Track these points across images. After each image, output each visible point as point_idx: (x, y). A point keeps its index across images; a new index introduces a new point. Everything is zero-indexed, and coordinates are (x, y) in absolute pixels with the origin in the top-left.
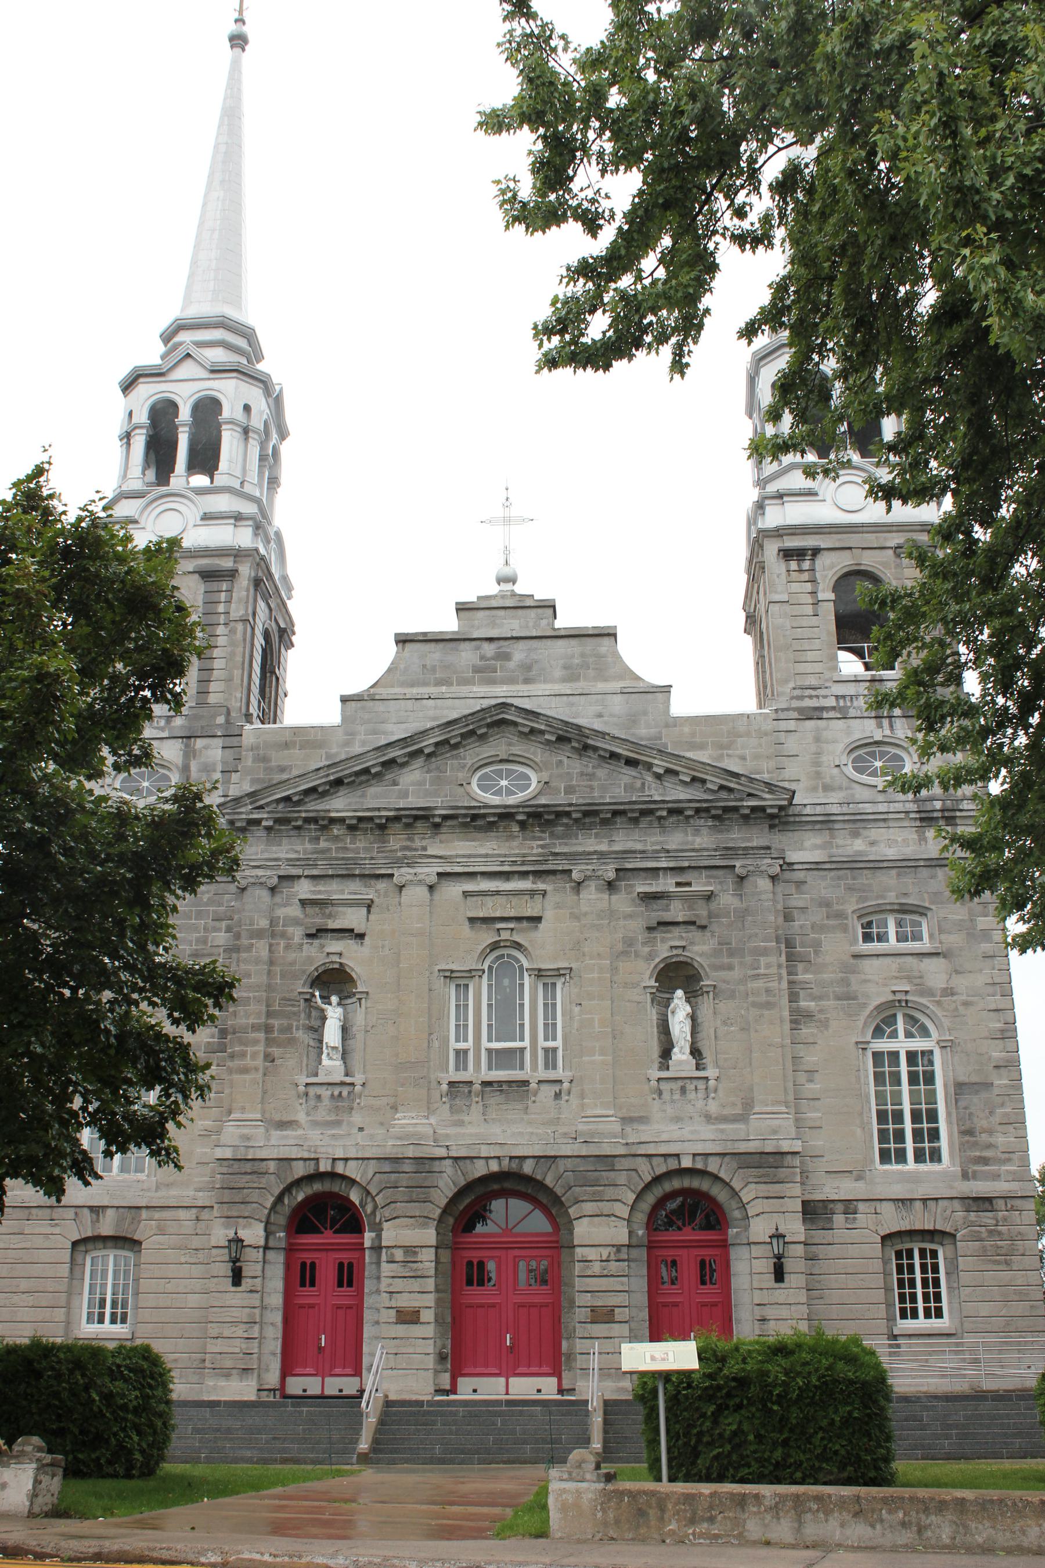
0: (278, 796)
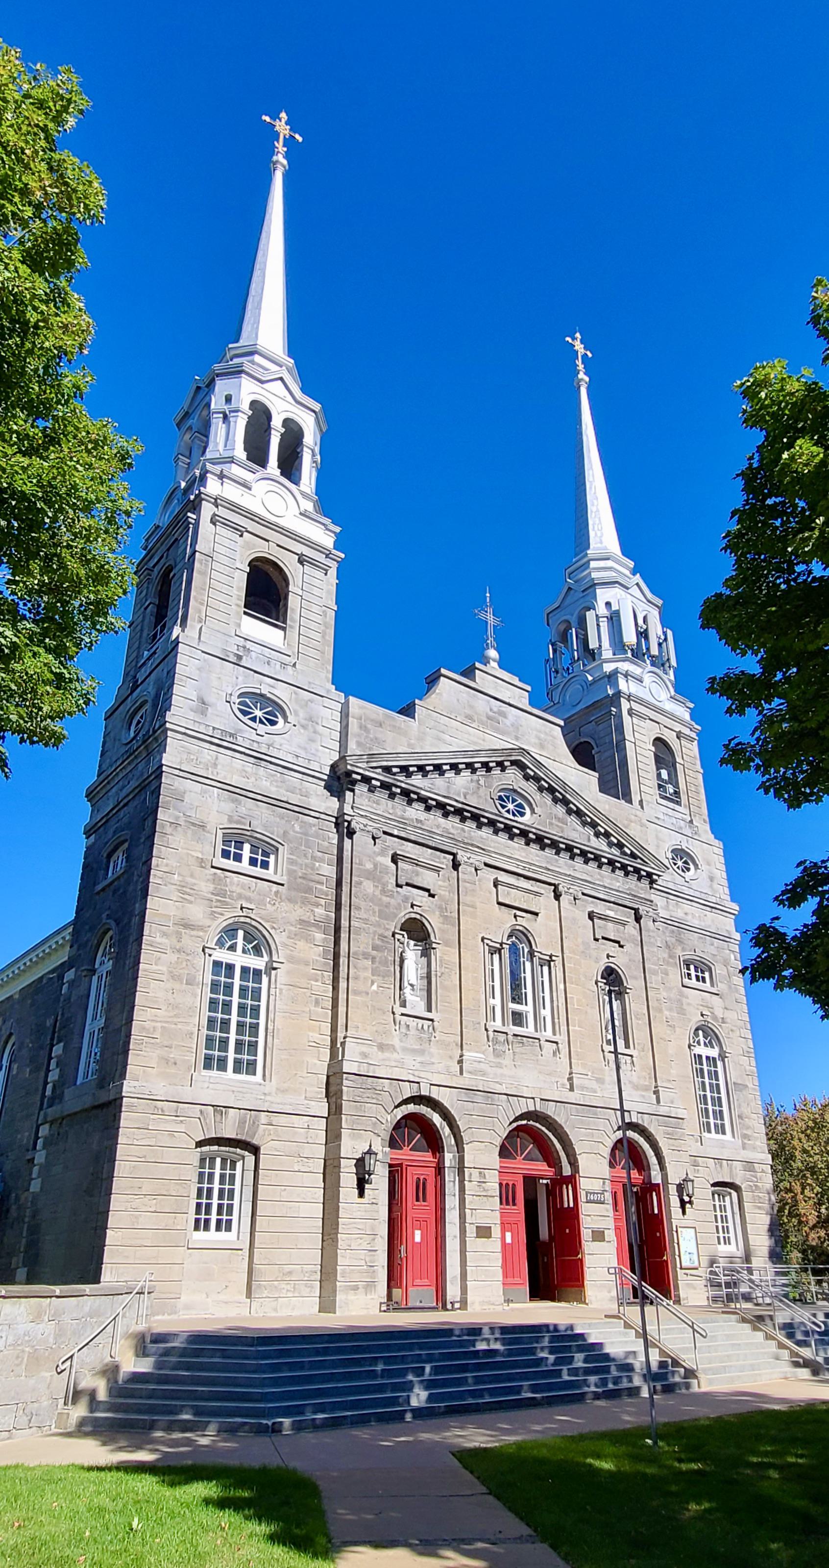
0: (385, 764)
